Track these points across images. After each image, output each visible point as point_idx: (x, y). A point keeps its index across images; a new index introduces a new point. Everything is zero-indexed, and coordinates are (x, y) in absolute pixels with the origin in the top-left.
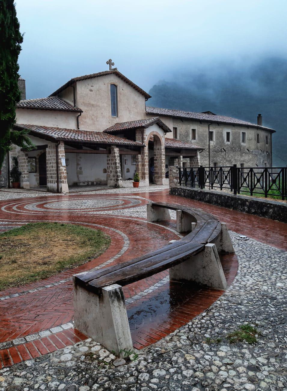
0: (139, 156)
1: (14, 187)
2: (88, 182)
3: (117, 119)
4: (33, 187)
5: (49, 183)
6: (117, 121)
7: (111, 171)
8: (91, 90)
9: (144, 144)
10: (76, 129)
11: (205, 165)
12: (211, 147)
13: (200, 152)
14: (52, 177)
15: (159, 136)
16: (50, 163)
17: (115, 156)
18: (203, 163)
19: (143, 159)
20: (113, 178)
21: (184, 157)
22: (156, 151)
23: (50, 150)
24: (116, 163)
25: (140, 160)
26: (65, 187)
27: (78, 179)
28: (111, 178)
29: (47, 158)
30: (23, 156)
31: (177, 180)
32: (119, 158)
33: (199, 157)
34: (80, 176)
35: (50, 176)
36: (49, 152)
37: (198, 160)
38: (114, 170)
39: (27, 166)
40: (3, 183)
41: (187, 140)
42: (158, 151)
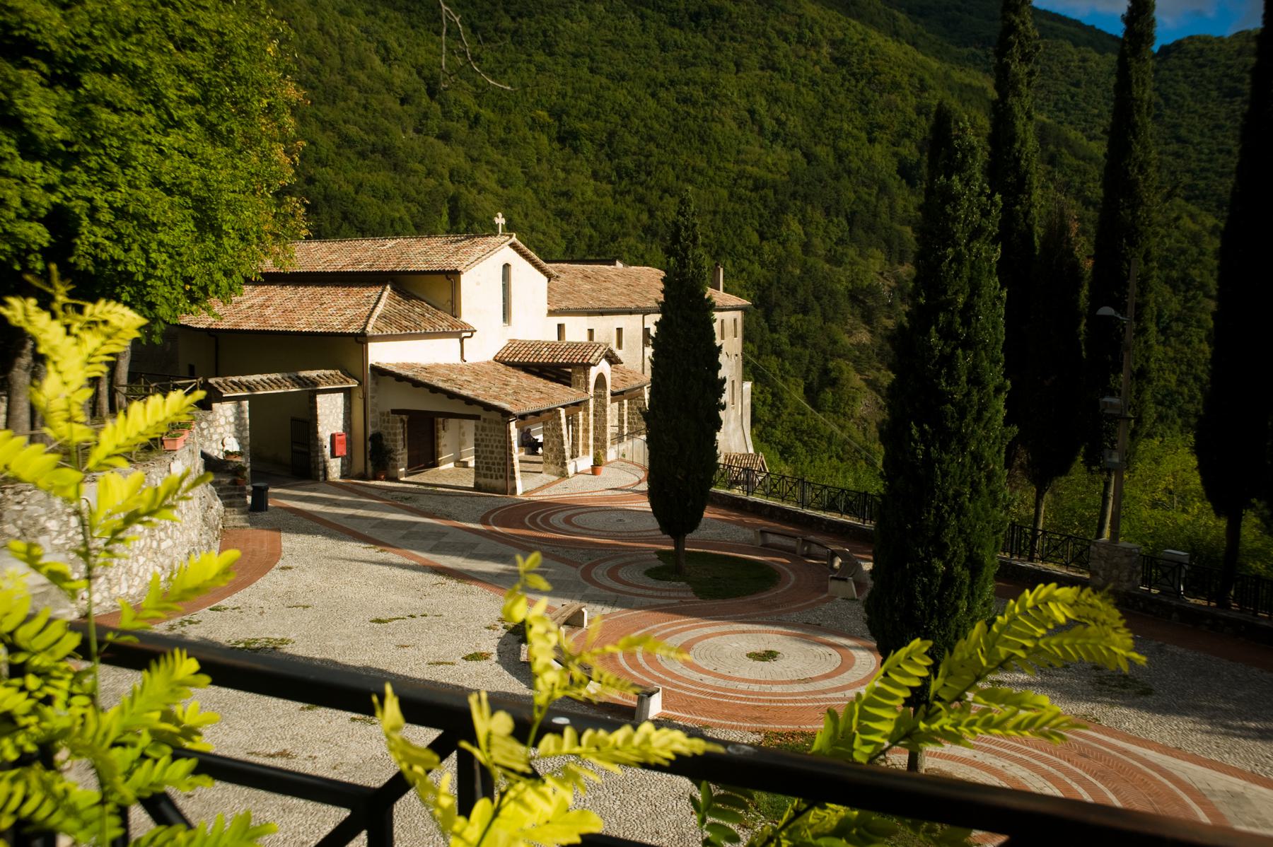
8: (478, 284)
19: (586, 420)
23: (486, 425)
24: (562, 436)
25: (581, 421)
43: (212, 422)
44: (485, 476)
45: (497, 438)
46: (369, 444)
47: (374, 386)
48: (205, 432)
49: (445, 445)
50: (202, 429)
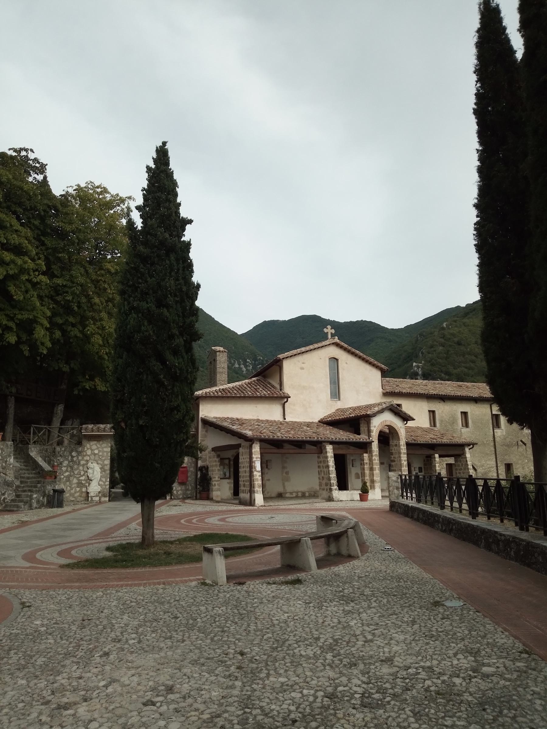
0: (366, 455)
1: (201, 499)
2: (297, 492)
3: (339, 402)
4: (225, 498)
6: (339, 405)
7: (323, 477)
8: (302, 368)
9: (371, 439)
10: (281, 419)
11: (489, 468)
12: (497, 439)
13: (469, 447)
14: (244, 485)
15: (395, 427)
16: (243, 467)
17: (327, 457)
18: (485, 465)
19: (371, 460)
20: (326, 488)
21: (440, 456)
22: (393, 448)
23: (243, 451)
24: (328, 467)
26: (259, 498)
27: (284, 487)
28: (322, 487)
29: (240, 461)
30: (214, 457)
31: (399, 491)
32: (333, 459)
33: (468, 455)
34: (286, 483)
36: (242, 453)
37: (467, 461)
38: (327, 476)
39: (219, 470)
40: (189, 492)
41: (454, 429)
42: (396, 448)
43: (81, 452)
46: (199, 473)
47: (204, 432)
48: (75, 459)
49: (269, 480)
50: (73, 457)
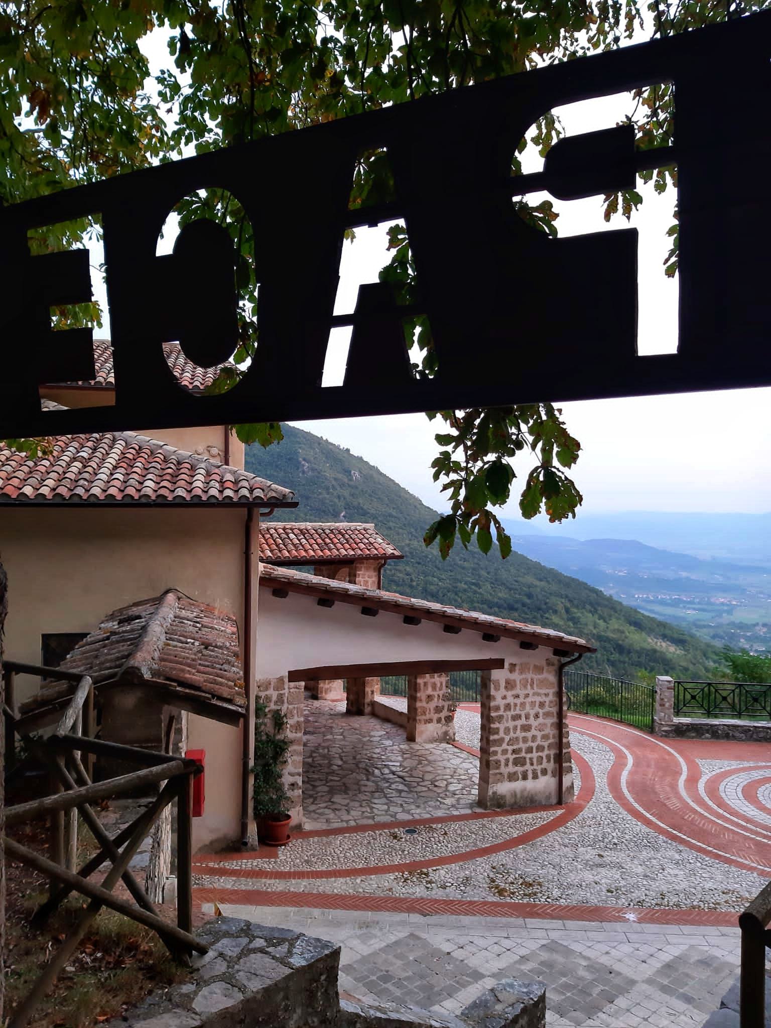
5: (499, 781)
16: (516, 717)
23: (516, 676)
28: (428, 717)
35: (507, 760)
38: (441, 693)
44: (512, 777)
45: (538, 699)
